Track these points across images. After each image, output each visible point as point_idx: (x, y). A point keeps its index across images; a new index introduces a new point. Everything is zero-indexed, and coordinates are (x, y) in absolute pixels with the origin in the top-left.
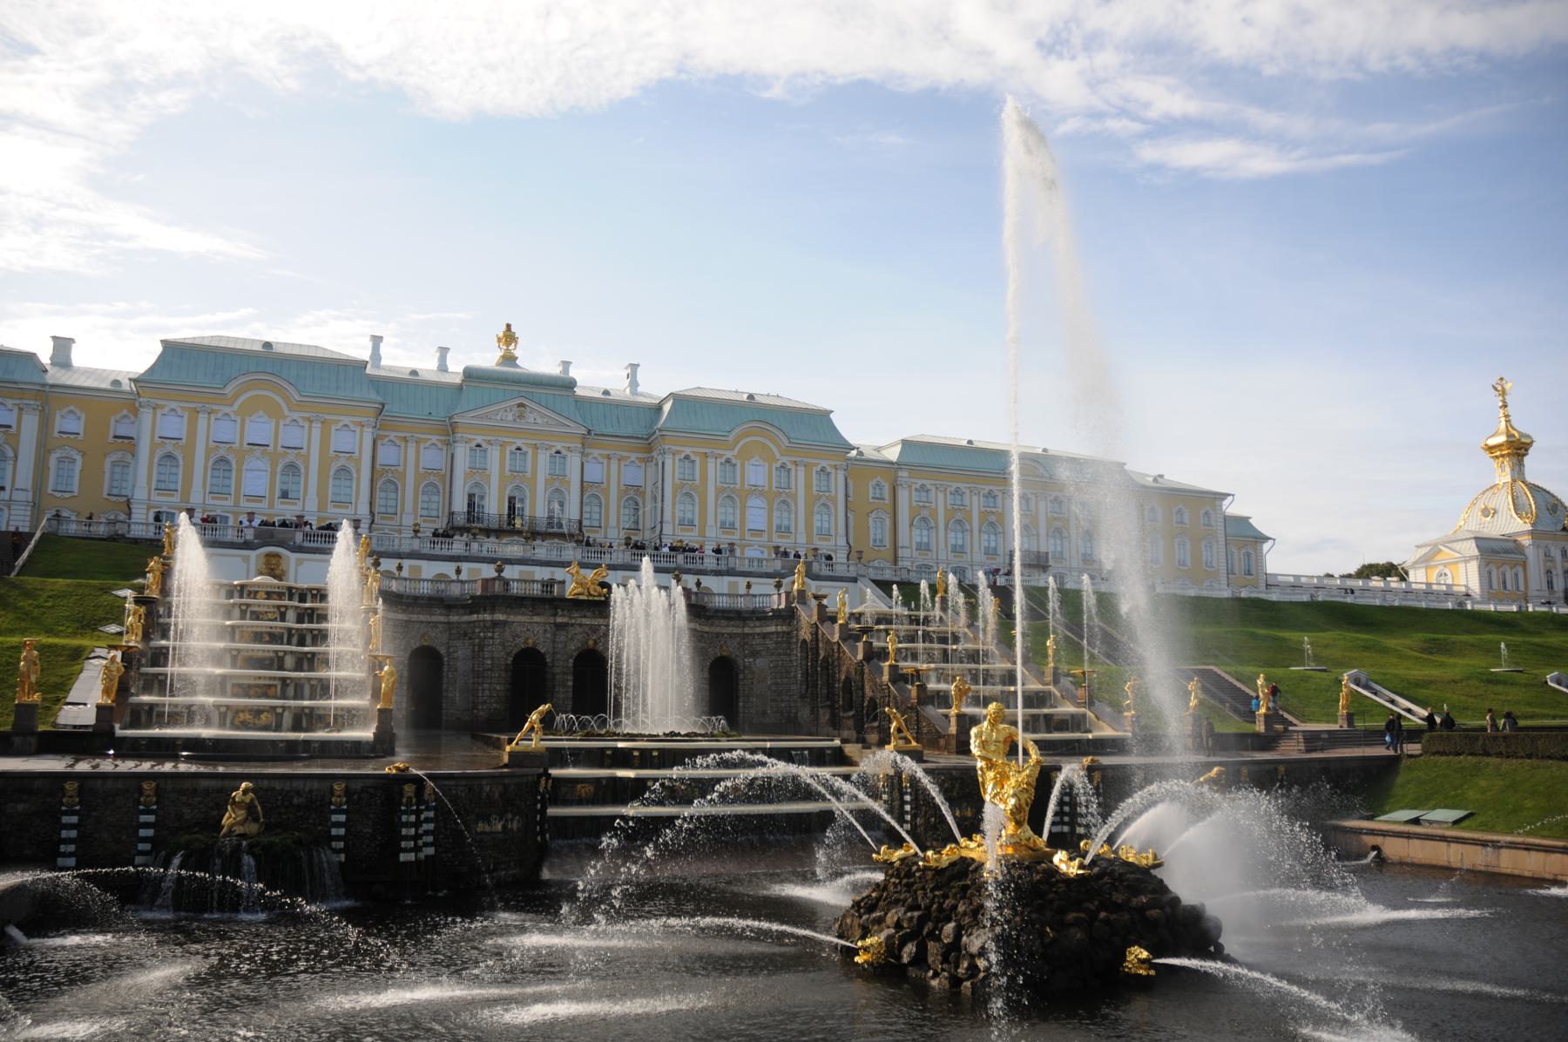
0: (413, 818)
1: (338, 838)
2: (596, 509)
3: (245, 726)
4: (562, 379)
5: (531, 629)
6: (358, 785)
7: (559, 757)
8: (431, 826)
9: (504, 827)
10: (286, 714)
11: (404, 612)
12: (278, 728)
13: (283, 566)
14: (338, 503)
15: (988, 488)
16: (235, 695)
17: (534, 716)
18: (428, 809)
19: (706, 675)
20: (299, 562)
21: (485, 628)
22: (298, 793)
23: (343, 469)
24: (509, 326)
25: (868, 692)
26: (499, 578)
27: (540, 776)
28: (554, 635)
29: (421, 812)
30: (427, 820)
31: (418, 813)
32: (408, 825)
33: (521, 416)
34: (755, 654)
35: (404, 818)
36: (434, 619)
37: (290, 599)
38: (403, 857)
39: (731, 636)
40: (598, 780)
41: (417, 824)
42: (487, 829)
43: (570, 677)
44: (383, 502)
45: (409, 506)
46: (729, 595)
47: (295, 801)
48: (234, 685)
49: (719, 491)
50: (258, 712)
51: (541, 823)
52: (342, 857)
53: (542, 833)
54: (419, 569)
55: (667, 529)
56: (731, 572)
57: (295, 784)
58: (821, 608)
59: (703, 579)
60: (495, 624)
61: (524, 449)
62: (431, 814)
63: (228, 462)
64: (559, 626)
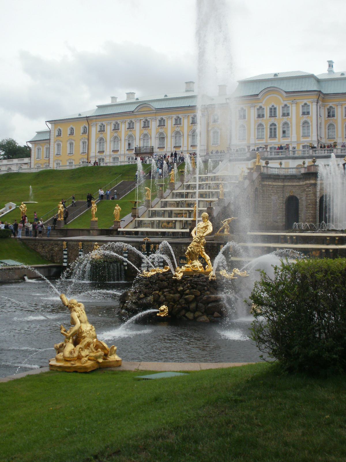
3: (165, 227)
11: (283, 182)
12: (175, 228)
14: (304, 136)
16: (174, 217)
21: (308, 187)
23: (306, 122)
36: (294, 184)
45: (340, 134)
50: (168, 222)
52: (126, 268)
60: (311, 185)
63: (263, 126)
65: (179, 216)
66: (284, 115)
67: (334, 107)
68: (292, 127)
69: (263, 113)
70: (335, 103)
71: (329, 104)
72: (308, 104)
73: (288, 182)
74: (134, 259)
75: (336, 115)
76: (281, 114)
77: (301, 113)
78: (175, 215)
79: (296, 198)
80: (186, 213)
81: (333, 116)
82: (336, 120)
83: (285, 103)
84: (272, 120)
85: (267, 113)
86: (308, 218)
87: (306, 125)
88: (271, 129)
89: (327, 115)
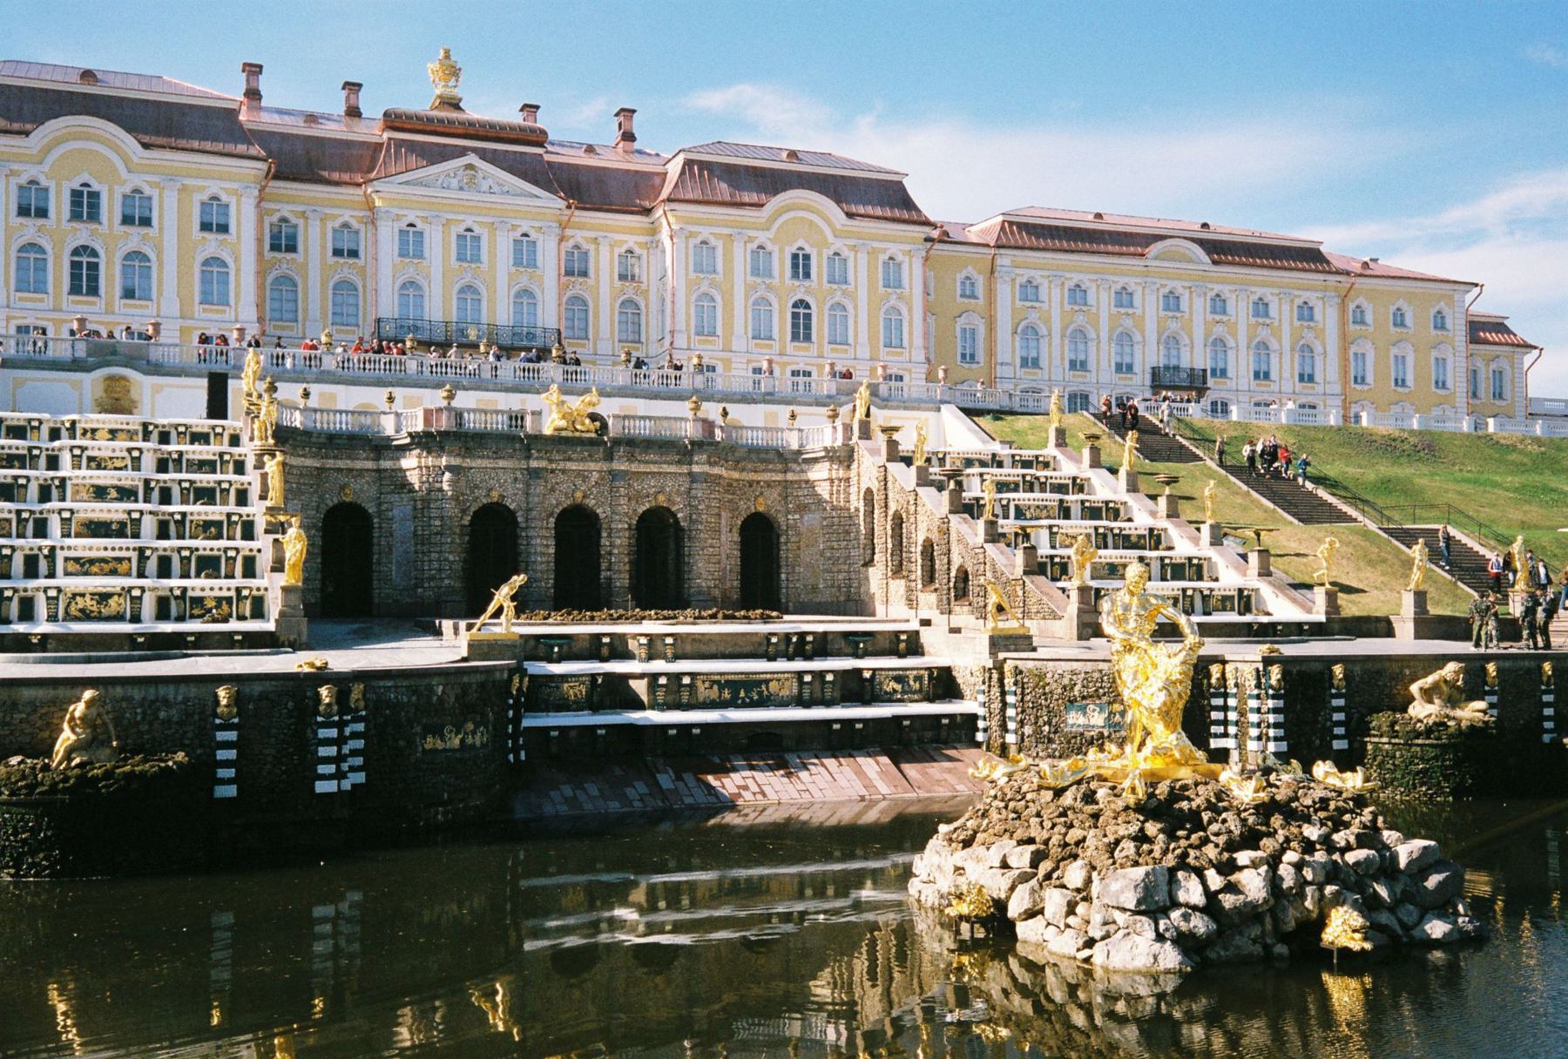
0: (333, 733)
1: (227, 764)
2: (582, 315)
3: (86, 616)
4: (522, 129)
5: (499, 479)
6: (257, 688)
7: (541, 647)
8: (359, 744)
9: (462, 741)
10: (147, 596)
13: (134, 394)
15: (1122, 281)
16: (67, 574)
17: (503, 595)
18: (356, 720)
19: (737, 538)
20: (157, 389)
22: (166, 702)
24: (447, 52)
25: (956, 561)
26: (449, 409)
27: (512, 671)
28: (528, 486)
29: (347, 723)
30: (355, 735)
31: (341, 725)
32: (328, 742)
33: (472, 184)
34: (802, 508)
35: (323, 733)
36: (359, 465)
37: (146, 438)
38: (322, 787)
39: (769, 484)
40: (593, 676)
41: (340, 741)
42: (440, 745)
43: (552, 542)
44: (277, 305)
46: (766, 429)
47: (162, 715)
48: (67, 559)
49: (751, 289)
50: (104, 597)
51: (515, 736)
53: (516, 751)
54: (333, 397)
55: (681, 341)
56: (769, 398)
57: (162, 690)
58: (892, 445)
59: (730, 407)
61: (477, 230)
62: (360, 727)
64: (534, 474)
65: (94, 569)
66: (127, 220)
67: (294, 221)
68: (161, 264)
69: (41, 204)
70: (301, 208)
71: (337, 216)
72: (224, 198)
73: (335, 458)
74: (273, 752)
75: (300, 247)
76: (118, 218)
77: (197, 226)
78: (72, 567)
79: (364, 511)
80: (129, 560)
81: (292, 248)
82: (306, 264)
83: (137, 181)
84: (82, 234)
85: (59, 205)
86: (432, 578)
87: (216, 269)
88: (75, 266)
89: (267, 246)
